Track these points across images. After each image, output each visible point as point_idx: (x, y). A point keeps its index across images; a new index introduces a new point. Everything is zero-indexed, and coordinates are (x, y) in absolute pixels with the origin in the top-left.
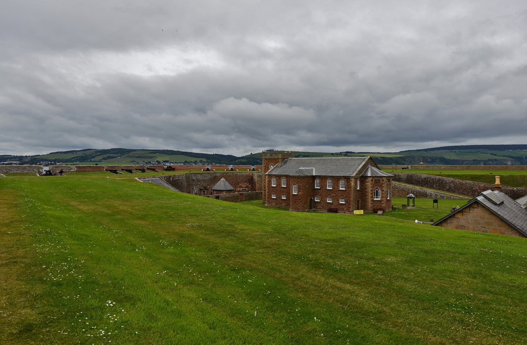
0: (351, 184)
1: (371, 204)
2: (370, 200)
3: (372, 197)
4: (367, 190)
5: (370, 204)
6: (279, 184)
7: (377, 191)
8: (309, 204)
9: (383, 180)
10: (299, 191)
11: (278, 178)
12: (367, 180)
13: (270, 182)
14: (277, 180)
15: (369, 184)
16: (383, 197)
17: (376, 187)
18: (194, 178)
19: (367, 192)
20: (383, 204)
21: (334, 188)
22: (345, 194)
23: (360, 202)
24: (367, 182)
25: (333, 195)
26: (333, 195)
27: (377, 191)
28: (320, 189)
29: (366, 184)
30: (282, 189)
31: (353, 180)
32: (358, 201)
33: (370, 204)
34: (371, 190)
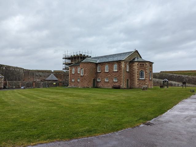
0: (121, 66)
1: (138, 82)
2: (136, 79)
3: (138, 77)
4: (134, 72)
5: (136, 82)
6: (76, 72)
7: (142, 73)
8: (92, 83)
9: (146, 65)
10: (85, 73)
12: (134, 65)
14: (75, 69)
15: (136, 66)
16: (146, 77)
17: (141, 69)
18: (37, 74)
20: (147, 82)
21: (109, 70)
23: (129, 81)
24: (134, 66)
26: (109, 75)
27: (142, 73)
28: (101, 72)
29: (134, 67)
31: (123, 63)
32: (128, 80)
33: (136, 82)
34: (137, 72)
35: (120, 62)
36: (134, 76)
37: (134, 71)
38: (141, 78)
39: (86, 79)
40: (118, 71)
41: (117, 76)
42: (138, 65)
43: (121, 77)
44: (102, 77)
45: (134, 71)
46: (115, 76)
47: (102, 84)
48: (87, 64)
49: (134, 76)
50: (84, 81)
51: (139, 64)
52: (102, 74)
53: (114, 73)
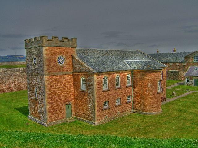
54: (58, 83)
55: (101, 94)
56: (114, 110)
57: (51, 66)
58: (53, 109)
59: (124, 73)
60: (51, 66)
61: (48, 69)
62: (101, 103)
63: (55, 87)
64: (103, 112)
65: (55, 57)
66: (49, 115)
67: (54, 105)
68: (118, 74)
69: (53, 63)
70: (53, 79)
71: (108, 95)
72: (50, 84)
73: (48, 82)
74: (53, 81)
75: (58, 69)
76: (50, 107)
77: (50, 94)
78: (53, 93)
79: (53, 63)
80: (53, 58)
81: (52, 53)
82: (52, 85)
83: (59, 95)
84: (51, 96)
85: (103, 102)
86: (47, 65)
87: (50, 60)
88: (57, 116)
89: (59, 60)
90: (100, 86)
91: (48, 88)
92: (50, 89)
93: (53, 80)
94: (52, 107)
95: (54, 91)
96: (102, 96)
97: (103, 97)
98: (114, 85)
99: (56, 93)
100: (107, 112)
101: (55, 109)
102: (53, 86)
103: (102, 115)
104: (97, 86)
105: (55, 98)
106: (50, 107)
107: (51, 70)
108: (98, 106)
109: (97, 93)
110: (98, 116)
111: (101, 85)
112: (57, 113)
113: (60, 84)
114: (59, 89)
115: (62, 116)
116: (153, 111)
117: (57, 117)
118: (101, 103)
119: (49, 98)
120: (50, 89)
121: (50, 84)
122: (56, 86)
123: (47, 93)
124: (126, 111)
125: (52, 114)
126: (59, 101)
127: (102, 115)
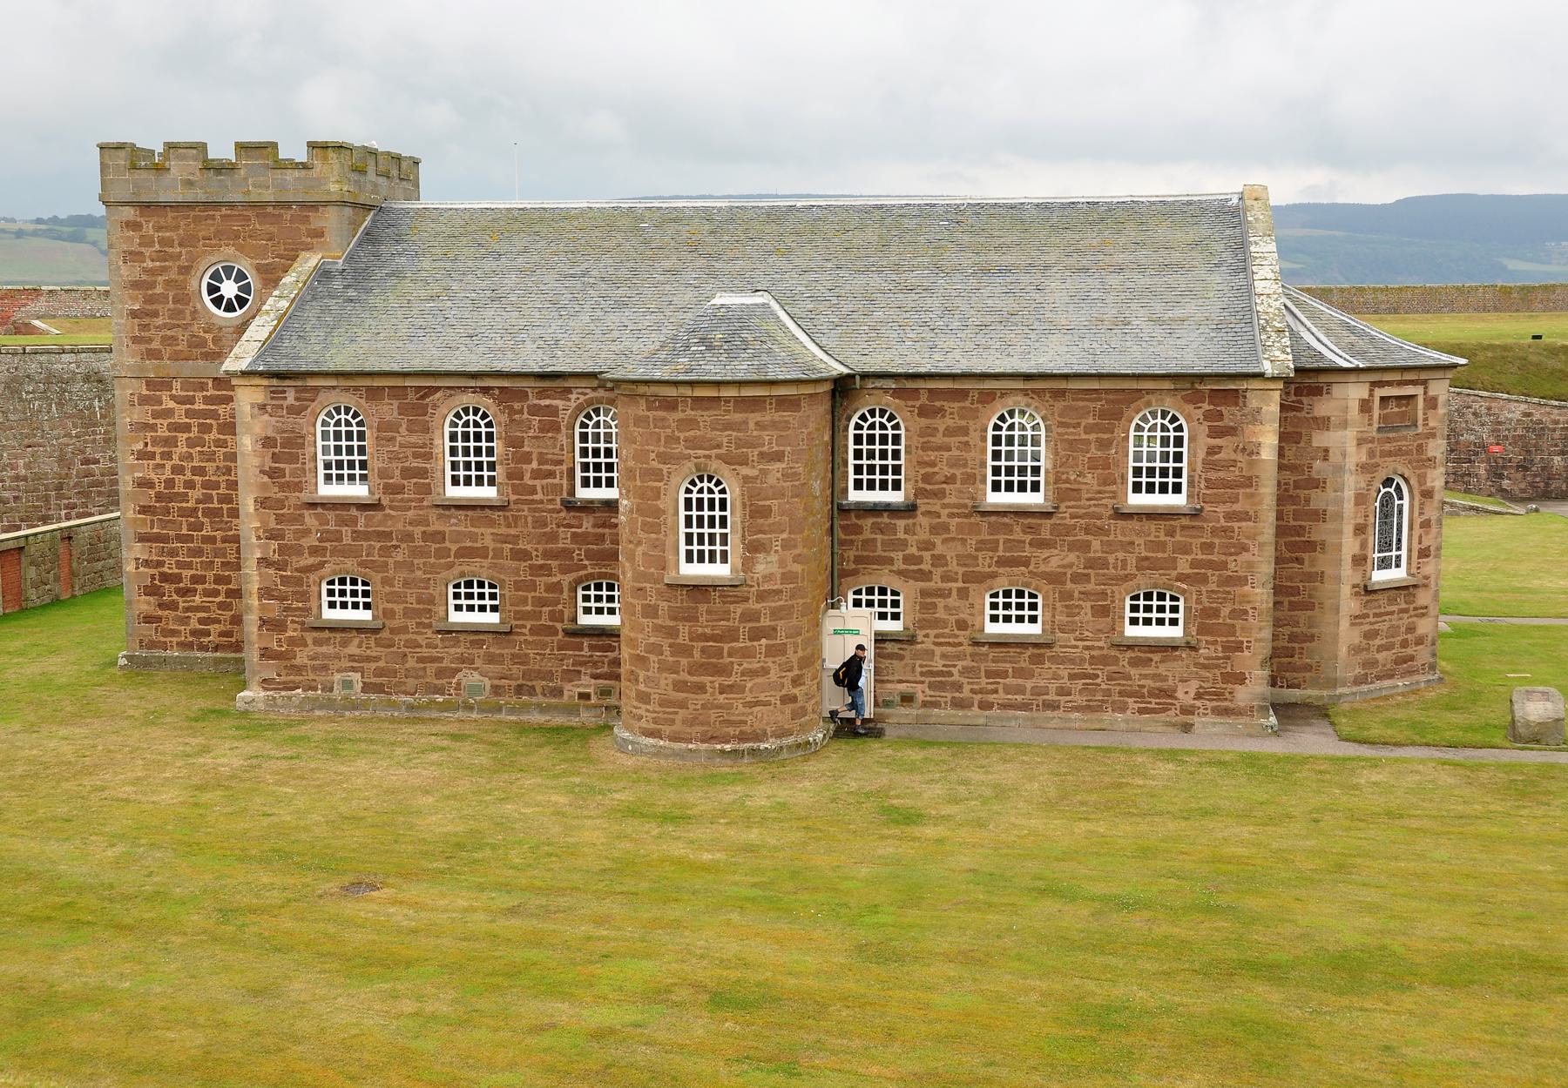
0: (1251, 451)
1: (1356, 619)
2: (1346, 590)
3: (1360, 560)
4: (1318, 500)
5: (1344, 624)
7: (1387, 501)
9: (1432, 403)
11: (389, 409)
12: (1322, 407)
13: (285, 451)
17: (1389, 467)
19: (1319, 516)
22: (1182, 552)
24: (1324, 423)
25: (1056, 559)
26: (1056, 559)
27: (1387, 501)
28: (909, 510)
29: (1320, 439)
30: (455, 525)
33: (1344, 624)
35: (1235, 397)
36: (1311, 546)
37: (1317, 484)
38: (1384, 564)
39: (770, 632)
40: (1196, 515)
41: (1183, 565)
42: (1365, 406)
43: (1242, 581)
44: (925, 576)
45: (1317, 484)
46: (1145, 564)
47: (938, 664)
48: (784, 403)
49: (1311, 546)
50: (747, 653)
51: (1380, 392)
52: (935, 530)
53: (1134, 524)
54: (205, 429)
55: (299, 519)
56: (426, 652)
57: (159, 321)
58: (165, 578)
59: (542, 393)
60: (159, 321)
61: (135, 340)
62: (299, 582)
63: (182, 448)
64: (317, 642)
65: (186, 270)
66: (144, 607)
67: (173, 553)
68: (469, 399)
69: (171, 306)
70: (173, 398)
71: (357, 535)
72: (153, 427)
73: (141, 414)
74: (169, 413)
75: (203, 343)
76: (147, 563)
77: (151, 485)
78: (170, 483)
79: (171, 306)
80: (173, 275)
81: (162, 241)
82: (163, 432)
83: (209, 499)
84: (159, 497)
85: (313, 577)
86: (134, 314)
87: (152, 285)
88: (194, 624)
89: (218, 289)
90: (287, 467)
91: (140, 446)
92: (152, 456)
93: (172, 404)
94: (160, 564)
95: (177, 470)
96: (307, 532)
97: (312, 541)
98: (423, 473)
99: (190, 485)
100: (353, 649)
101: (178, 578)
102: (170, 442)
103: (301, 658)
104: (256, 461)
105: (184, 513)
106: (147, 563)
107: (155, 345)
108: (266, 593)
109: (262, 503)
110: (266, 654)
111: (293, 459)
112: (197, 609)
113: (214, 435)
114: (210, 467)
115: (228, 634)
116: (643, 724)
117: (194, 633)
118: (299, 582)
119: (144, 510)
120: (152, 456)
121: (153, 427)
122: (191, 443)
123: (129, 478)
124: (558, 692)
125: (161, 606)
126: (212, 540)
127: (301, 658)
